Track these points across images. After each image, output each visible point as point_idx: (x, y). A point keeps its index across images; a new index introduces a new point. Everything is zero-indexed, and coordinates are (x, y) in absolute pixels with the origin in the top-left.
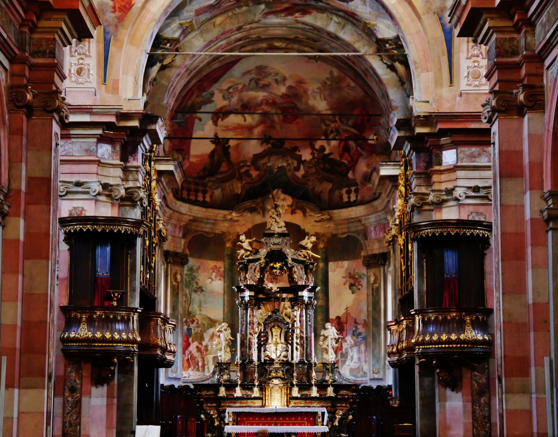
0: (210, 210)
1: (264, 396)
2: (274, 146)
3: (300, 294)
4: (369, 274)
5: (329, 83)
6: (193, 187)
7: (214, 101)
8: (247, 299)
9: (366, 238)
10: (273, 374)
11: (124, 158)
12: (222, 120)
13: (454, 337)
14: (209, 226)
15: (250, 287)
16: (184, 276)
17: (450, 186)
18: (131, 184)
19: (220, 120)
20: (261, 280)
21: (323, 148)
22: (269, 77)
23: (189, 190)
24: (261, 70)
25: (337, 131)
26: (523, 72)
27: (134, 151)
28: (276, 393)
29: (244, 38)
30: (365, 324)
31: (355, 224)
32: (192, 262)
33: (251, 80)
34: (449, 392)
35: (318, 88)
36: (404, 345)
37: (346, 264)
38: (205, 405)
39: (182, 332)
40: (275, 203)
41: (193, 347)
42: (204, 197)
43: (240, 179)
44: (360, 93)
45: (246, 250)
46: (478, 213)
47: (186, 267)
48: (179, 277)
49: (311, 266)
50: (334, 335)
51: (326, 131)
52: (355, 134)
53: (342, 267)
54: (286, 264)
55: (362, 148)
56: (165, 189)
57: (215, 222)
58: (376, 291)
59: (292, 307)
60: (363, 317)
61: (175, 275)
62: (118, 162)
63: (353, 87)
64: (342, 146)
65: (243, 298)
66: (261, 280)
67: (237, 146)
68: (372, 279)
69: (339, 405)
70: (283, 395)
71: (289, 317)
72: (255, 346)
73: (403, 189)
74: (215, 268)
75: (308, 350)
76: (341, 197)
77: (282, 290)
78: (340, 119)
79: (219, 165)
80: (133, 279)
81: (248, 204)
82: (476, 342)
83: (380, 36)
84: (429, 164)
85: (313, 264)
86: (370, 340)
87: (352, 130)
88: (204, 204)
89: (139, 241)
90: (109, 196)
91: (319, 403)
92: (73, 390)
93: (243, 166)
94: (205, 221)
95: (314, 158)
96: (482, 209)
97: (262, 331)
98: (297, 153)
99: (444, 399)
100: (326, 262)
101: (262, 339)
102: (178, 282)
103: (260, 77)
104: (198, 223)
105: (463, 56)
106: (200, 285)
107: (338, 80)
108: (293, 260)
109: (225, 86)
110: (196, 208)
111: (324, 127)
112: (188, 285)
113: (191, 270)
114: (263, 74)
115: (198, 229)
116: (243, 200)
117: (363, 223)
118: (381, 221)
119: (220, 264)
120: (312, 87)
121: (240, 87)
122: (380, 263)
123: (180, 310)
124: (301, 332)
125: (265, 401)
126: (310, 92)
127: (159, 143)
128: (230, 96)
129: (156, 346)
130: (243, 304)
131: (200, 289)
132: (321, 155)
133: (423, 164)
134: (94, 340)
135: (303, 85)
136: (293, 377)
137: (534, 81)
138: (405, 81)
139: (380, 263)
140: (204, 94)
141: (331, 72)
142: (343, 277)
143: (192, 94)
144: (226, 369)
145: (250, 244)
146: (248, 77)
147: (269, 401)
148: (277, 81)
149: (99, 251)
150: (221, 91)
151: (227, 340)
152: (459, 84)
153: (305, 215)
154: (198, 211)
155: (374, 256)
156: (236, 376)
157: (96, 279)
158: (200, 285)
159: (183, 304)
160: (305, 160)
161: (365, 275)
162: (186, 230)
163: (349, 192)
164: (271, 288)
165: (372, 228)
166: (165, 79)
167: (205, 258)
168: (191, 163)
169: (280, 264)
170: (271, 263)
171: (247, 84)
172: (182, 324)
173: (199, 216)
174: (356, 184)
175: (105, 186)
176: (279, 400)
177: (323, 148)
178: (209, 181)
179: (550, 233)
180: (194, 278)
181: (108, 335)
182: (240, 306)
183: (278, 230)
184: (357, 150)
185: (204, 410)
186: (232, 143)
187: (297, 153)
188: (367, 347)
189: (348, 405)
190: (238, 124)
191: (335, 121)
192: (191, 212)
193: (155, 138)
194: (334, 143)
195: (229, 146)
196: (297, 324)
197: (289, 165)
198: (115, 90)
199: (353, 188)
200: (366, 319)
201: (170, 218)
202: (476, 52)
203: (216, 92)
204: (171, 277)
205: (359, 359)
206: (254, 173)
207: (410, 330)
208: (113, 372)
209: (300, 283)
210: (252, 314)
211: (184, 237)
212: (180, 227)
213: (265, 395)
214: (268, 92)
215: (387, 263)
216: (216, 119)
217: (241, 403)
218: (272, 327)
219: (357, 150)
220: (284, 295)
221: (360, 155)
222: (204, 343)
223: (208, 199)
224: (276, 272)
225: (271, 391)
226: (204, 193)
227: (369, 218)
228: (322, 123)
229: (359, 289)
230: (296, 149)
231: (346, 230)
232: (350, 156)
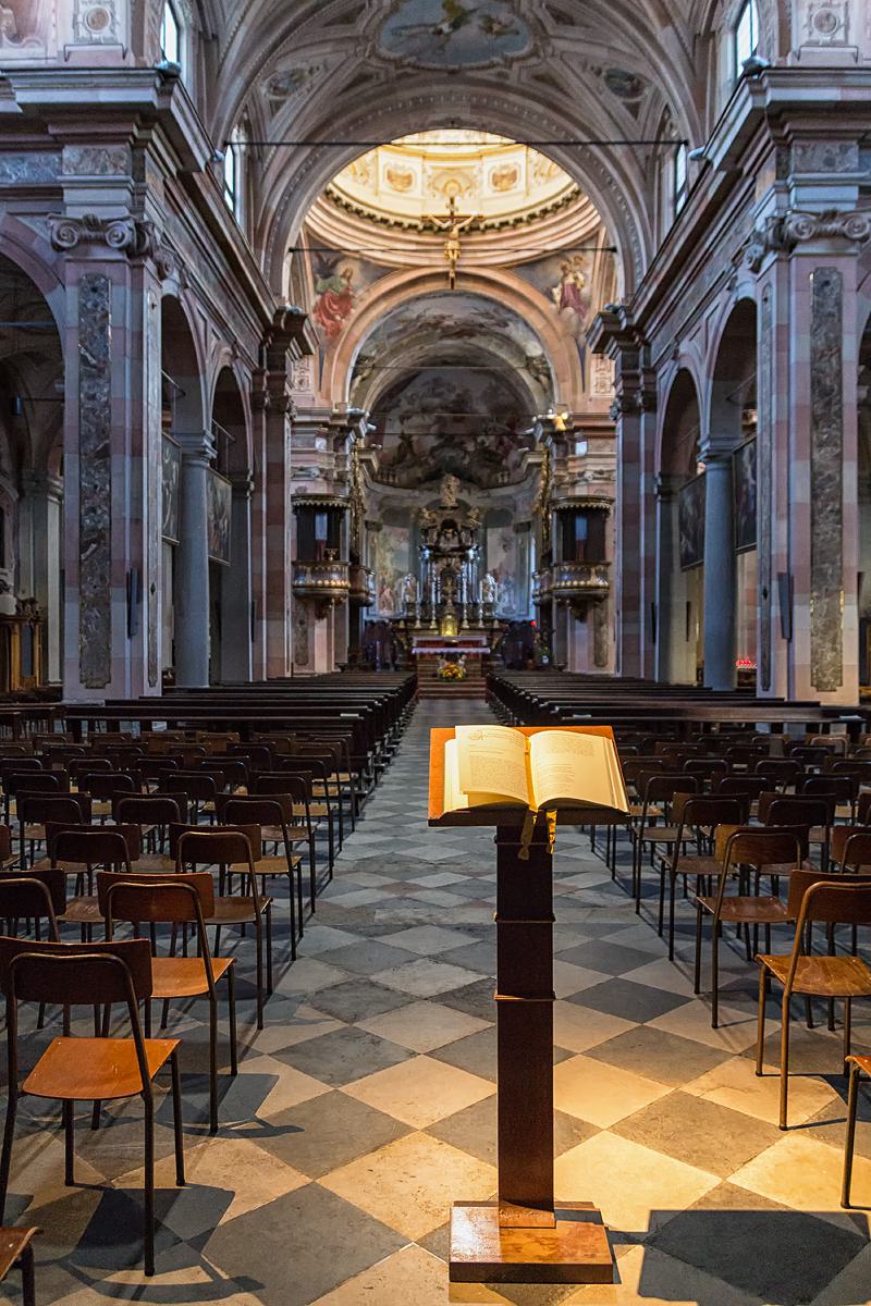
2: (446, 440)
8: (427, 556)
9: (515, 510)
11: (336, 450)
13: (582, 583)
15: (429, 548)
17: (581, 470)
18: (341, 469)
21: (483, 442)
24: (435, 380)
25: (494, 429)
26: (642, 381)
27: (343, 444)
30: (514, 575)
32: (386, 529)
34: (577, 623)
36: (546, 589)
37: (500, 530)
41: (387, 592)
43: (421, 465)
44: (512, 399)
46: (602, 491)
48: (376, 541)
54: (457, 530)
57: (403, 499)
59: (461, 562)
60: (512, 570)
62: (332, 452)
66: (438, 542)
67: (418, 441)
68: (520, 541)
72: (434, 590)
73: (545, 473)
74: (402, 534)
77: (453, 550)
79: (404, 456)
80: (344, 540)
81: (428, 485)
82: (598, 587)
83: (529, 354)
84: (566, 453)
86: (518, 586)
87: (508, 429)
88: (394, 486)
89: (348, 512)
90: (325, 478)
92: (302, 623)
96: (605, 488)
99: (573, 629)
100: (485, 528)
105: (593, 369)
107: (495, 390)
109: (409, 394)
113: (385, 535)
116: (424, 482)
119: (405, 530)
120: (476, 394)
127: (361, 437)
129: (361, 591)
133: (561, 454)
134: (316, 586)
137: (650, 388)
141: (491, 383)
145: (430, 515)
148: (449, 391)
149: (318, 519)
150: (406, 398)
152: (589, 392)
153: (470, 492)
154: (390, 491)
155: (522, 524)
156: (418, 612)
157: (317, 544)
162: (381, 506)
163: (502, 476)
174: (508, 470)
175: (322, 471)
177: (483, 442)
179: (659, 504)
181: (327, 582)
183: (450, 504)
186: (414, 438)
193: (359, 435)
194: (492, 438)
197: (458, 455)
198: (328, 397)
202: (603, 367)
205: (510, 601)
206: (432, 462)
207: (550, 579)
208: (330, 610)
211: (379, 510)
220: (455, 553)
221: (511, 448)
222: (395, 589)
223: (397, 481)
226: (394, 476)
230: (463, 443)
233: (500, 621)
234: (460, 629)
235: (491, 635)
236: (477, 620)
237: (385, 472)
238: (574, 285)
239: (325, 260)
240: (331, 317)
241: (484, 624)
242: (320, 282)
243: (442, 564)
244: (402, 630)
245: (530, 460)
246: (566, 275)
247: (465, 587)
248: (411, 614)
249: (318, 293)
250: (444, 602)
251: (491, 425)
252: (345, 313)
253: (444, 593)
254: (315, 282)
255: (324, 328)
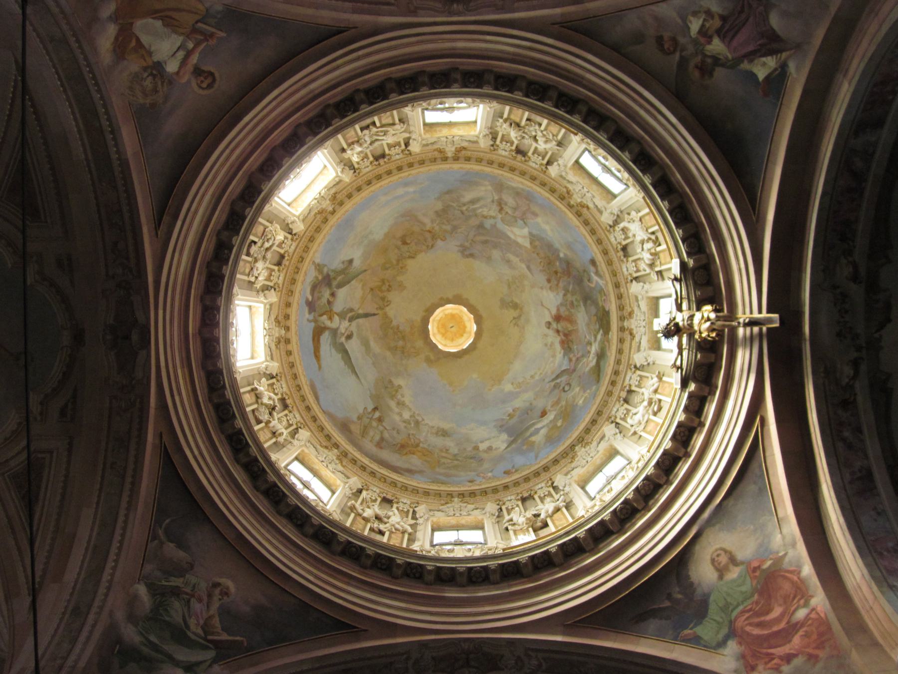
238: (719, 32)
239: (667, 604)
240: (794, 628)
242: (706, 630)
246: (717, 61)
249: (722, 644)
252: (801, 592)
254: (695, 641)
255: (798, 662)
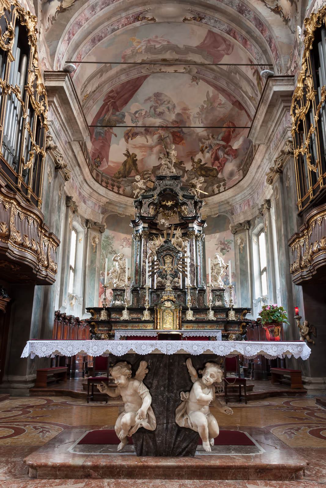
0: (122, 197)
1: (155, 319)
3: (190, 225)
4: (236, 239)
5: (205, 106)
6: (110, 182)
7: (125, 122)
8: (140, 231)
9: (233, 214)
10: (166, 298)
12: (132, 139)
14: (121, 209)
16: (102, 241)
19: (130, 139)
20: (155, 216)
21: (200, 161)
22: (163, 105)
23: (107, 183)
24: (157, 95)
25: (211, 146)
28: (167, 316)
29: (141, 16)
31: (224, 206)
32: (108, 232)
33: (151, 108)
35: (198, 113)
37: (217, 235)
38: (96, 329)
39: (99, 281)
40: (168, 150)
42: (119, 191)
45: (141, 189)
47: (103, 234)
48: (97, 240)
49: (200, 204)
50: (222, 264)
51: (202, 148)
52: (223, 146)
53: (215, 238)
55: (228, 155)
56: (67, 130)
58: (242, 250)
61: (94, 238)
63: (224, 104)
64: (213, 157)
65: (137, 231)
66: (155, 216)
68: (239, 241)
69: (231, 329)
70: (175, 318)
71: (180, 247)
74: (126, 239)
75: (199, 278)
76: (213, 191)
78: (212, 136)
79: (129, 172)
85: (201, 202)
87: (223, 143)
88: (118, 193)
91: (211, 326)
93: (146, 174)
94: (119, 205)
95: (194, 168)
97: (155, 260)
98: (183, 165)
101: (155, 267)
102: (96, 244)
103: (157, 105)
104: (113, 206)
106: (114, 249)
108: (184, 196)
109: (133, 111)
110: (111, 193)
111: (201, 145)
112: (105, 248)
114: (159, 102)
115: (113, 210)
117: (230, 203)
118: (245, 199)
120: (194, 111)
121: (144, 113)
122: (245, 228)
123: (97, 264)
124: (192, 259)
125: (157, 324)
126: (191, 118)
128: (136, 121)
130: (138, 237)
131: (115, 252)
132: (199, 165)
135: (187, 112)
136: (185, 301)
138: (289, 18)
139: (245, 228)
140: (117, 113)
142: (216, 245)
143: (108, 110)
144: (121, 295)
145: (144, 183)
146: (149, 104)
147: (161, 325)
148: (168, 109)
150: (130, 114)
151: (122, 269)
154: (112, 196)
155: (241, 224)
158: (114, 249)
159: (100, 261)
160: (188, 170)
161: (232, 241)
162: (104, 211)
163: (218, 187)
164: (163, 225)
165: (238, 206)
166: (64, 20)
167: (119, 231)
168: (109, 166)
169: (171, 203)
170: (163, 202)
171: (148, 111)
172: (99, 274)
173: (114, 200)
174: (224, 180)
176: (170, 323)
177: (200, 161)
178: (122, 181)
180: (109, 244)
182: (135, 239)
184: (224, 157)
185: (95, 334)
186: (139, 158)
187: (183, 165)
188: (236, 292)
189: (241, 329)
190: (143, 144)
191: (209, 139)
192: (107, 196)
195: (137, 160)
196: (188, 254)
199: (222, 184)
200: (235, 272)
201: (90, 196)
203: (126, 114)
204: (90, 239)
209: (190, 216)
210: (145, 243)
211: (103, 213)
212: (99, 206)
213: (157, 318)
214: (162, 119)
215: (251, 228)
216: (127, 137)
217: (132, 327)
218: (164, 256)
219: (224, 157)
220: (175, 232)
221: (227, 159)
223: (121, 192)
224: (168, 213)
225: (163, 314)
226: (119, 187)
227: (236, 199)
228: (200, 142)
229: (228, 251)
231: (217, 212)
232: (219, 163)
233: (239, 311)
234: (183, 322)
235: (226, 330)
236: (205, 310)
237: (110, 182)
241: (215, 315)
243: (159, 242)
244: (103, 322)
245: (277, 88)
247: (188, 269)
248: (118, 303)
250: (161, 288)
251: (207, 142)
253: (162, 275)
